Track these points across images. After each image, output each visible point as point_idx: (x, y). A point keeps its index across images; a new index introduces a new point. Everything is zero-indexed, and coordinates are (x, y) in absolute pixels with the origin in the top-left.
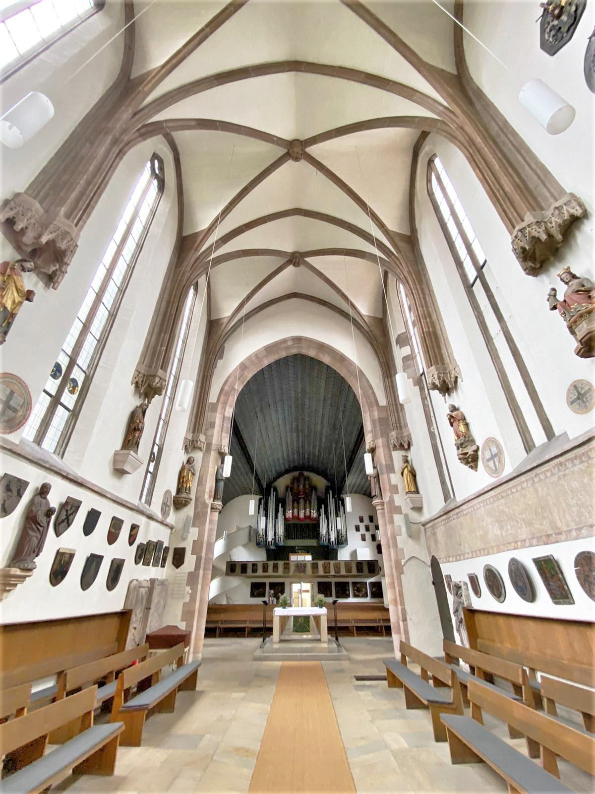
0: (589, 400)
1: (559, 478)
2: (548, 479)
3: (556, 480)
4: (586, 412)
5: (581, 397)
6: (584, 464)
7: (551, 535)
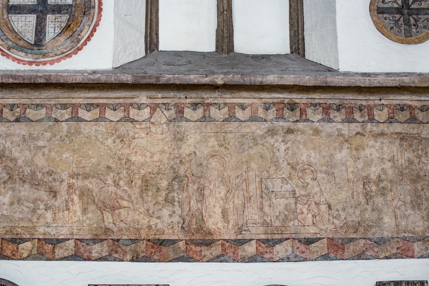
0: (420, 25)
1: (272, 132)
2: (236, 124)
3: (259, 132)
4: (402, 42)
5: (406, 11)
6: (353, 125)
7: (174, 242)
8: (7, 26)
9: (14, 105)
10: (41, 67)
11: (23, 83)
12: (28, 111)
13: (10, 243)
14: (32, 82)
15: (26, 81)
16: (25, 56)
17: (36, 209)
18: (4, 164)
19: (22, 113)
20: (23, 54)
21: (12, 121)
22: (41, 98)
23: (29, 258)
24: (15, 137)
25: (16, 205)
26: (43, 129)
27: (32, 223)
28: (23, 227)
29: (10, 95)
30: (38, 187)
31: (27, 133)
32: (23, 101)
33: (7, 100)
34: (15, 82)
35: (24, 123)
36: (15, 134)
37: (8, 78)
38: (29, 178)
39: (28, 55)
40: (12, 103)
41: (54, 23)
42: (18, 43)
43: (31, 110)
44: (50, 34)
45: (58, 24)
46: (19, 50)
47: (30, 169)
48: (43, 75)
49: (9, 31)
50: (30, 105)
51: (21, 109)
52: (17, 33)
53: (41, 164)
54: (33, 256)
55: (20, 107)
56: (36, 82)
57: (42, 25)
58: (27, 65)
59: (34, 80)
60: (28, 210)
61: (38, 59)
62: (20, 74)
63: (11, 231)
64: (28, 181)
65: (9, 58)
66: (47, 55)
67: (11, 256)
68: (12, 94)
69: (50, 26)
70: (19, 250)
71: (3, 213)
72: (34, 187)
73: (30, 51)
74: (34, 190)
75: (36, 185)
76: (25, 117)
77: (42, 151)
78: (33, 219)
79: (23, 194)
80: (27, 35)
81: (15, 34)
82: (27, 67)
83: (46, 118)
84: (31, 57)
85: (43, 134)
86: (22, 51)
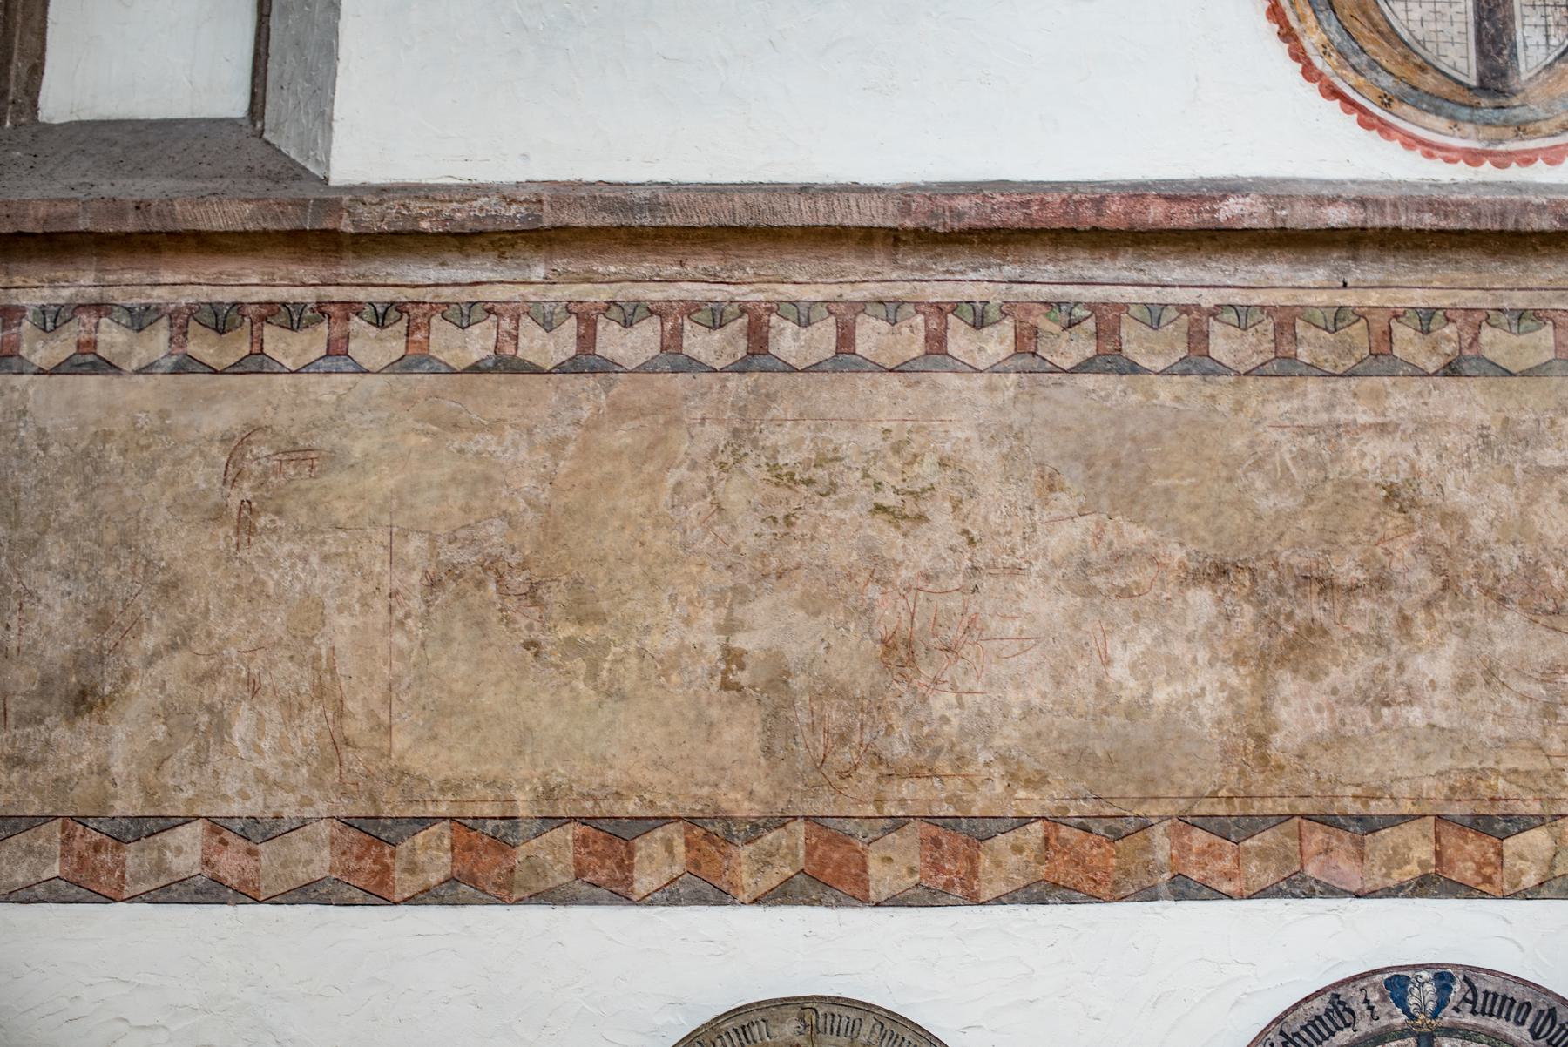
8: (1369, 18)
9: (1431, 312)
10: (1514, 173)
11: (1475, 232)
12: (1487, 334)
13: (1471, 835)
14: (1510, 225)
15: (1487, 224)
16: (1451, 132)
17: (1556, 705)
18: (1419, 533)
19: (1465, 344)
20: (1442, 123)
21: (1431, 371)
22: (1531, 289)
23: (1545, 891)
24: (1449, 433)
25: (1479, 689)
26: (1552, 403)
27: (1548, 756)
28: (1515, 771)
29: (1412, 277)
30: (1556, 621)
31: (1493, 418)
32: (1466, 298)
33: (1402, 294)
34: (1443, 224)
35: (1478, 381)
36: (1450, 420)
37: (1418, 211)
38: (1520, 586)
39: (1460, 125)
40: (1422, 305)
41: (1540, 11)
42: (1415, 83)
43: (1497, 331)
44: (1532, 50)
45: (1558, 15)
46: (1425, 106)
47: (1519, 552)
48: (1550, 201)
49: (1376, 36)
50: (1490, 313)
51: (1460, 329)
52: (1406, 44)
53: (1559, 533)
54: (1559, 881)
55: (1454, 322)
56: (1523, 227)
57: (1500, 16)
58: (1462, 163)
59: (1517, 221)
60: (1526, 706)
61: (1501, 141)
62: (1461, 197)
63: (1470, 789)
64: (1516, 597)
65: (1389, 137)
66: (1531, 127)
67: (1478, 884)
68: (1417, 272)
69: (1527, 21)
70: (1506, 860)
71: (1433, 722)
72: (1542, 620)
73: (1467, 111)
74: (1543, 631)
75: (1546, 613)
76: (1478, 358)
77: (1557, 484)
78: (1547, 741)
79: (1501, 646)
80: (1449, 53)
81: (1400, 49)
82: (1461, 172)
83: (1557, 364)
84: (1473, 135)
85: (1553, 423)
86: (1437, 112)
